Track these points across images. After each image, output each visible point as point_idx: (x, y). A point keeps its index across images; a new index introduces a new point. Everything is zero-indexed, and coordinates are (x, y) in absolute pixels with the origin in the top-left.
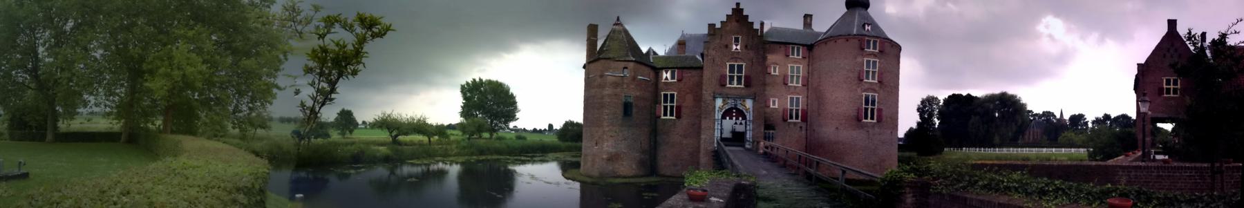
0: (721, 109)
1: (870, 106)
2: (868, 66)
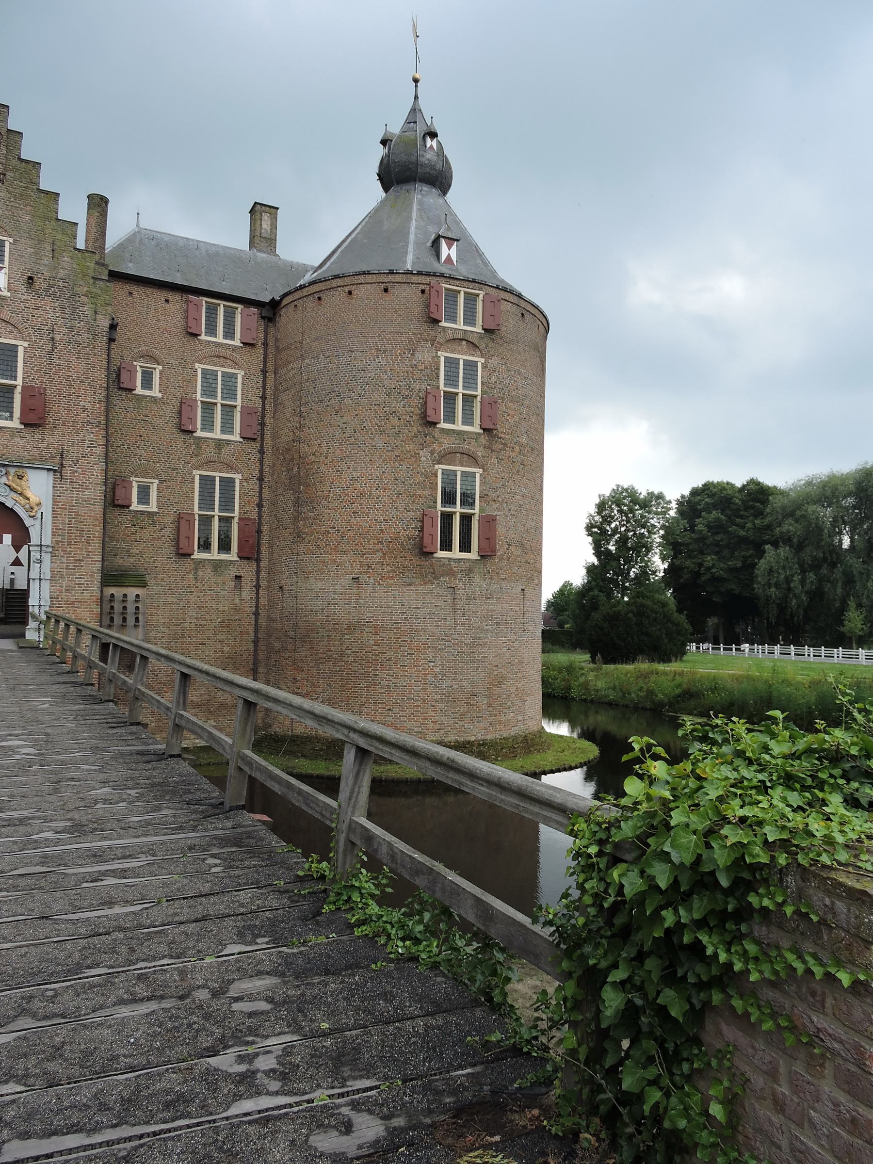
2: (451, 379)
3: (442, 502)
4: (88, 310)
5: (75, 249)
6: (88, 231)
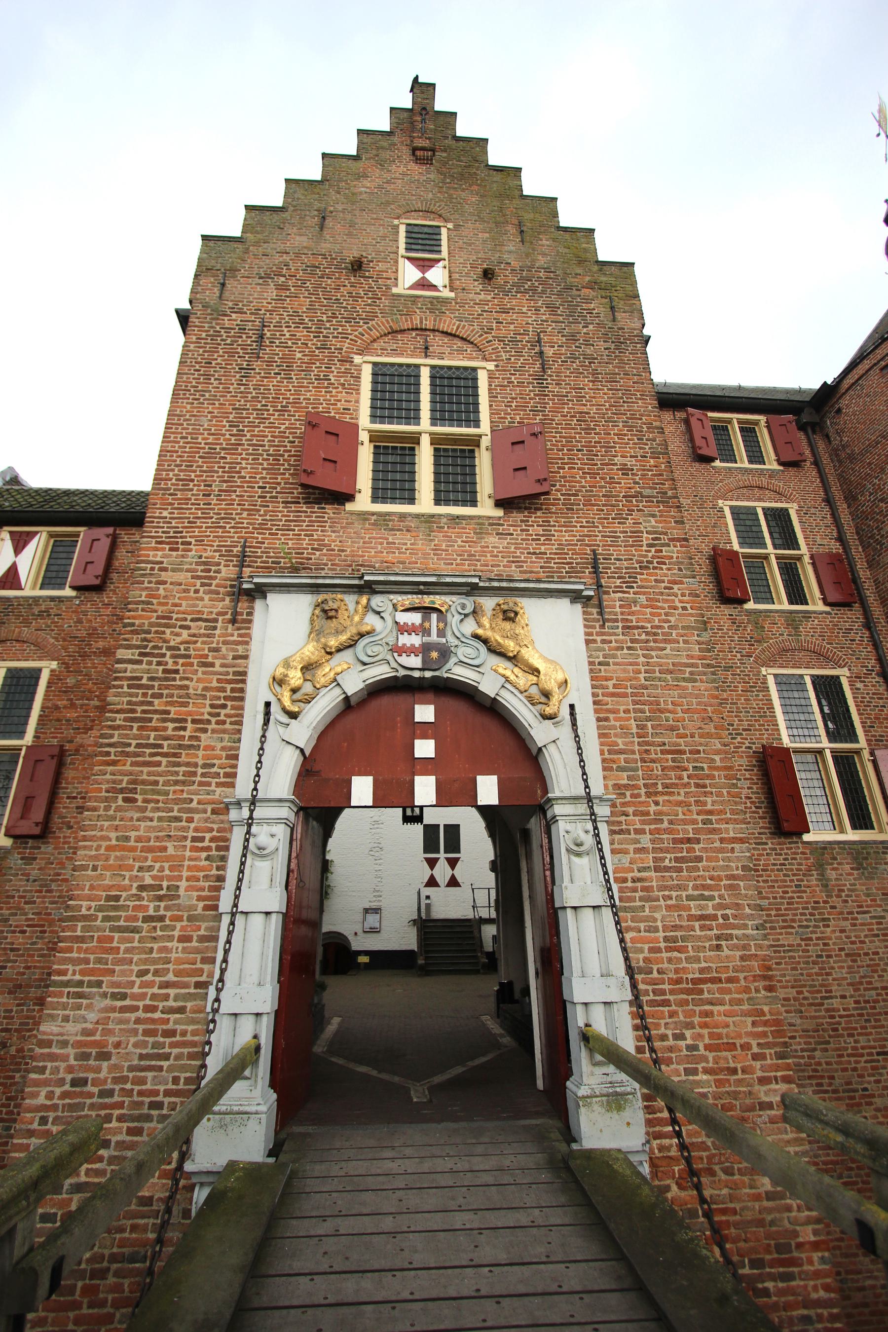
4: (598, 306)
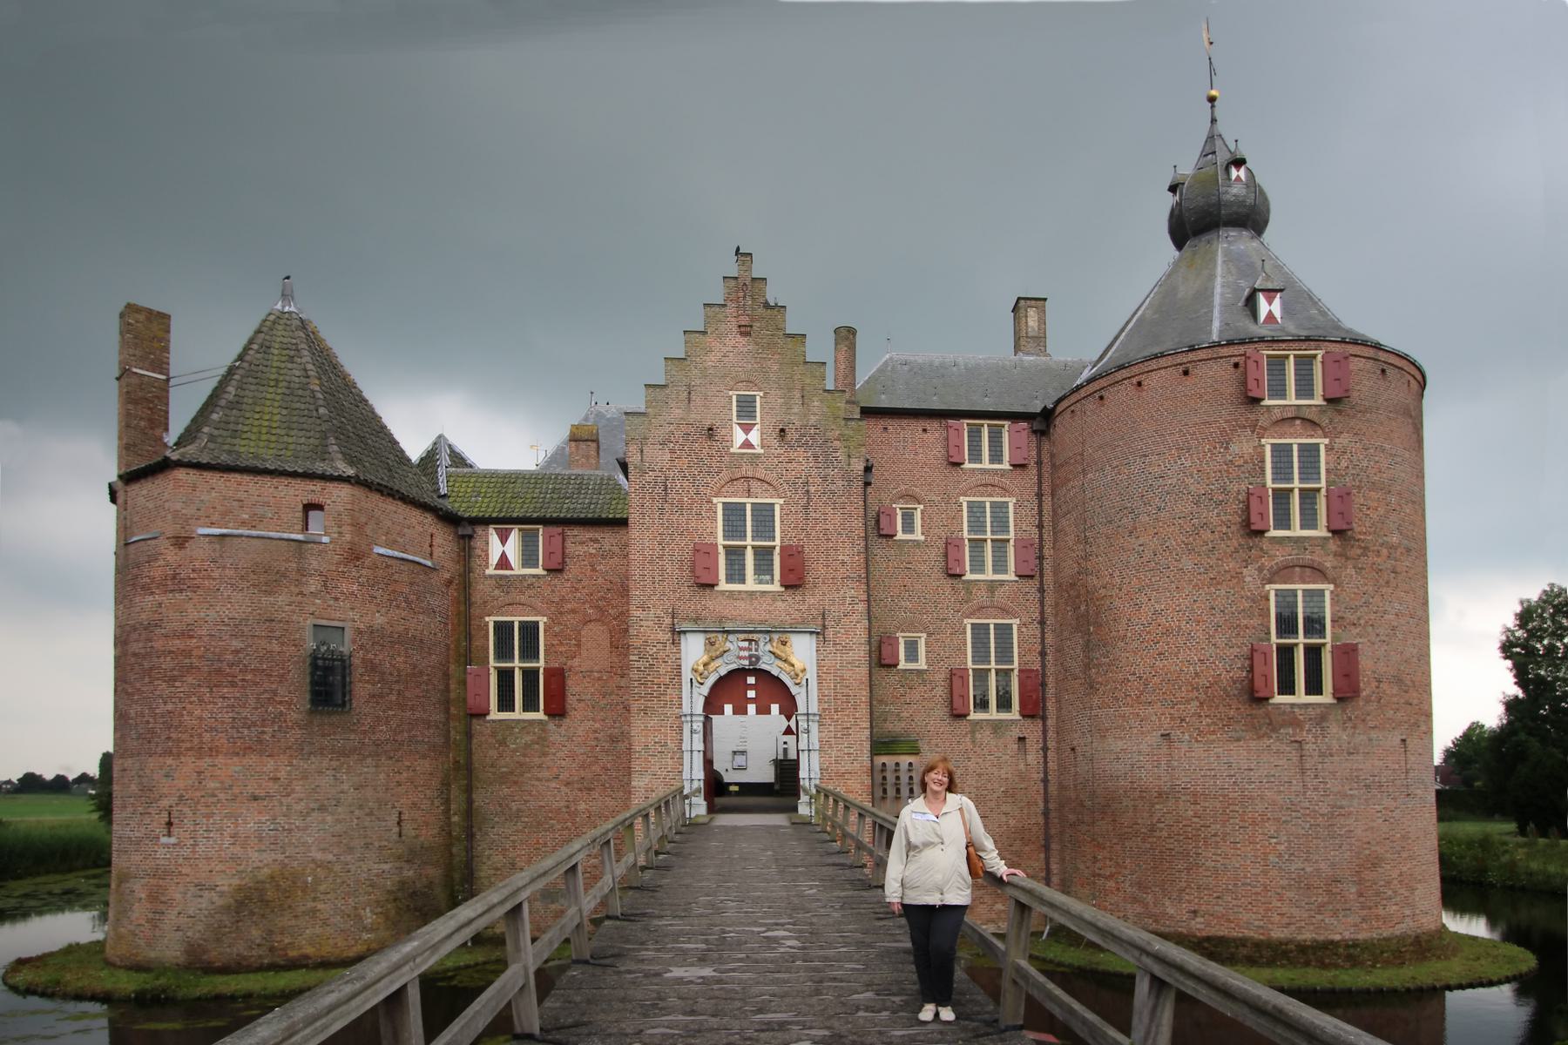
0: (700, 674)
1: (1301, 639)
2: (1282, 472)
3: (1277, 633)
5: (825, 391)
6: (836, 369)
